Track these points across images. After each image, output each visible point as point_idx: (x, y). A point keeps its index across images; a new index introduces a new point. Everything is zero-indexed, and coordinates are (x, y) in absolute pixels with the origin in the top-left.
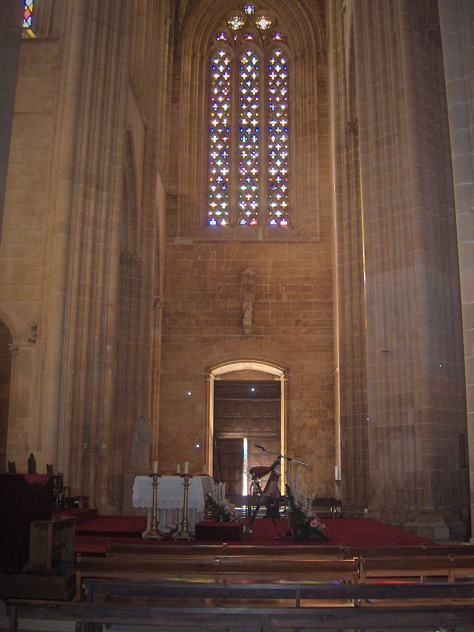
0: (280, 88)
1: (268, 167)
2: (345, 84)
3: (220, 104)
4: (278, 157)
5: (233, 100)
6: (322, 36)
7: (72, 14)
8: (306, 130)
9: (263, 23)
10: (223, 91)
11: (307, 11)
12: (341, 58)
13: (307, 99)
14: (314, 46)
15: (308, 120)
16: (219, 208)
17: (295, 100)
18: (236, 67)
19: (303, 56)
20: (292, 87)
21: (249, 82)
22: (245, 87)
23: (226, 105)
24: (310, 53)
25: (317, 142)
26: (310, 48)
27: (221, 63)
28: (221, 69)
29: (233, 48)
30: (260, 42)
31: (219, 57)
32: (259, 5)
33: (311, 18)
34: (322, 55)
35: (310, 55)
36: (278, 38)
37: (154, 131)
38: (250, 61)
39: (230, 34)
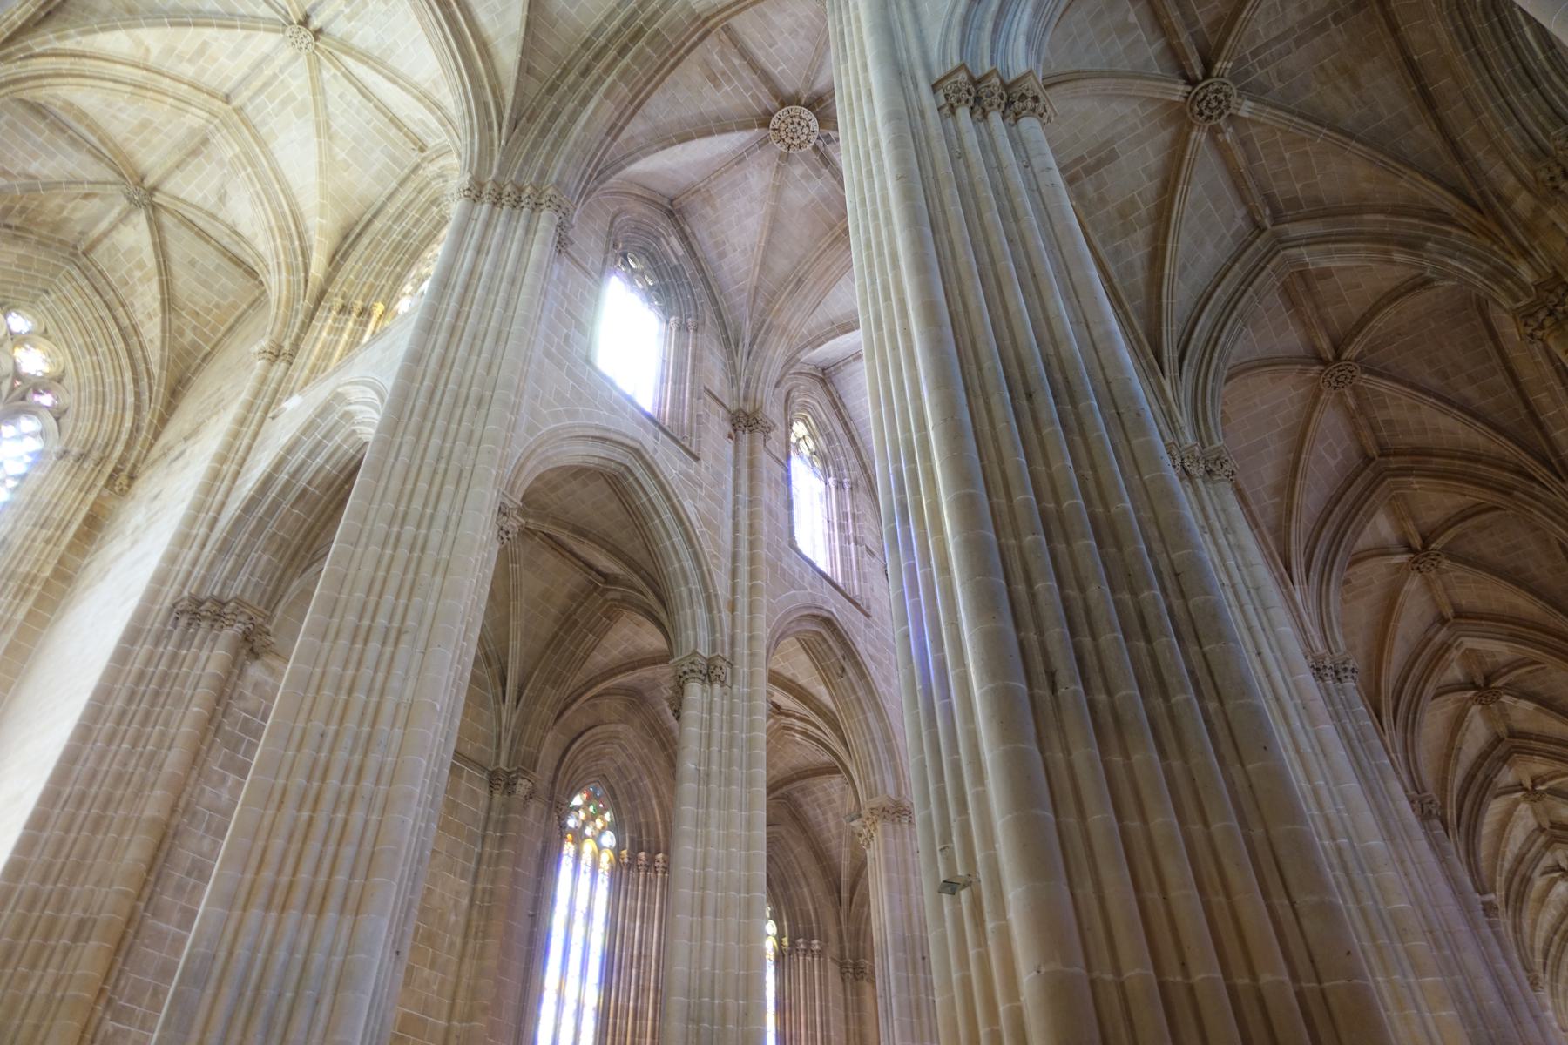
11: (138, 395)
15: (23, 569)
24: (101, 462)
33: (138, 409)
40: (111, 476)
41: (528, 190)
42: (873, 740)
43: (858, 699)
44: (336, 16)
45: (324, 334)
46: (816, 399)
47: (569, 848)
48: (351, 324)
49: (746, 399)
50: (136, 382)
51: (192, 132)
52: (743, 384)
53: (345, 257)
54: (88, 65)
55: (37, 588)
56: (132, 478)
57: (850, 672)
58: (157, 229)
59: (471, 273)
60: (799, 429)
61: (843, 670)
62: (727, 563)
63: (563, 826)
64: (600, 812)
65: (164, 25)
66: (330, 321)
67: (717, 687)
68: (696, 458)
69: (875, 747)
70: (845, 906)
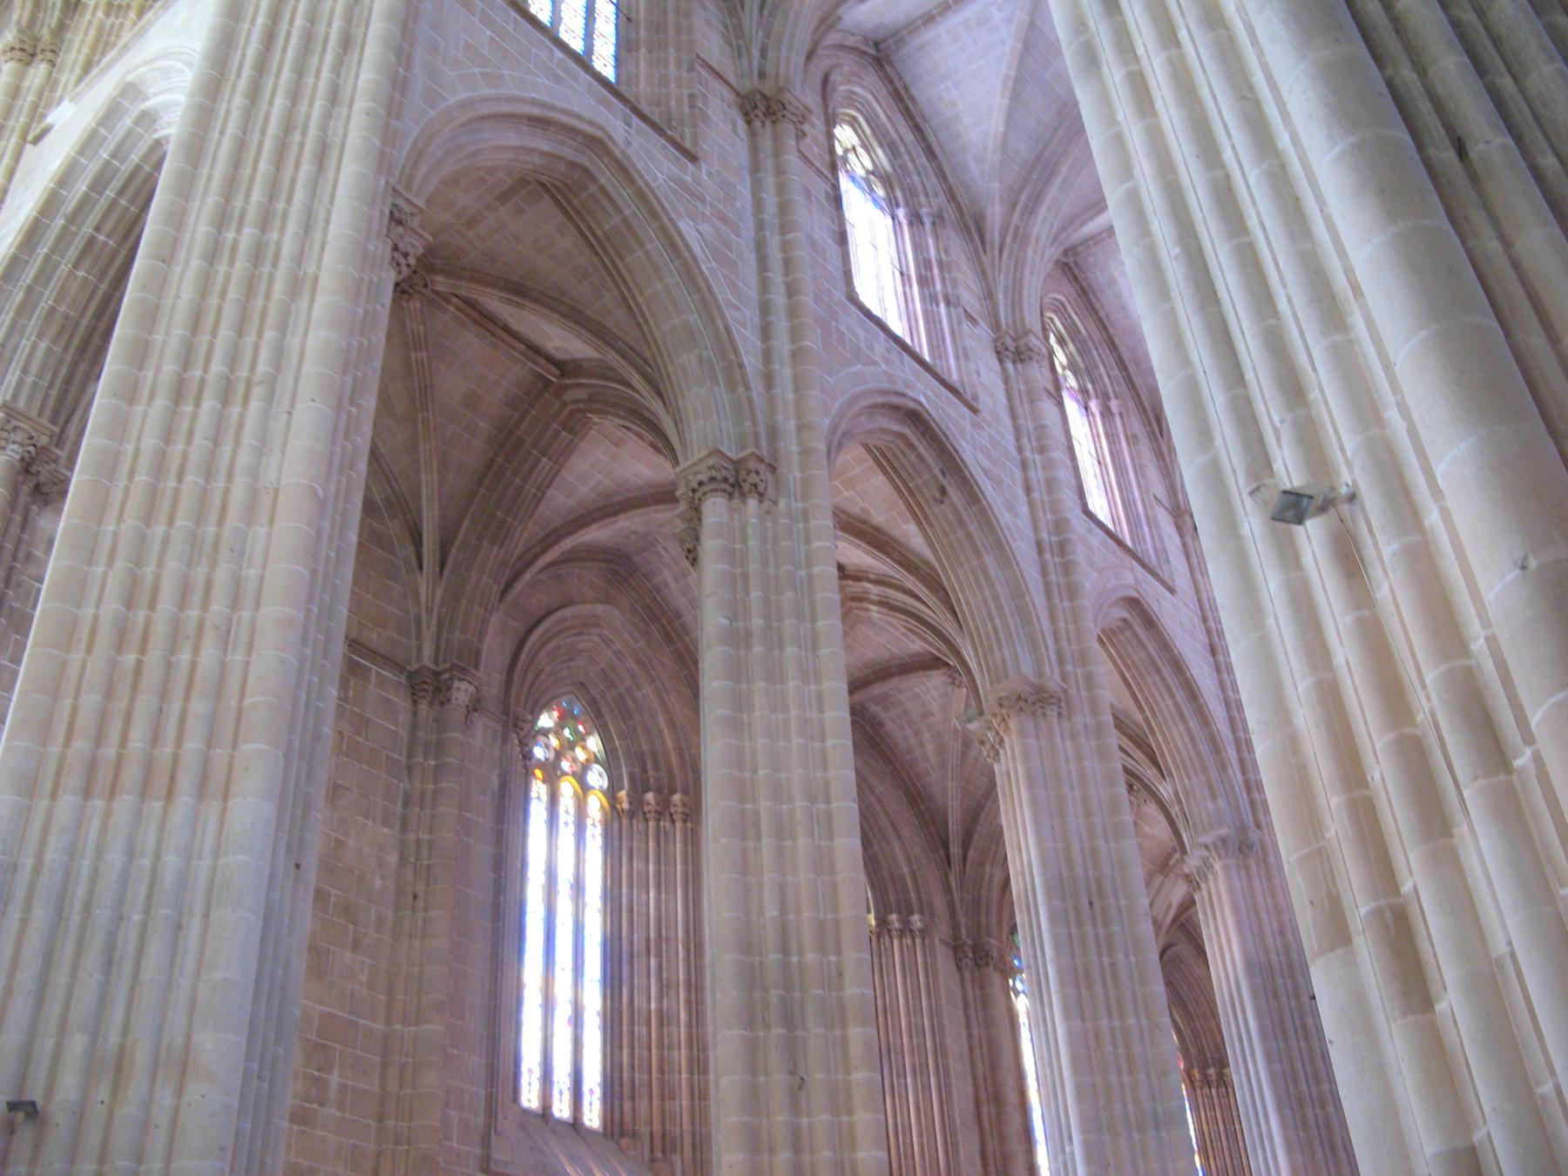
42: (996, 597)
43: (969, 536)
46: (865, 88)
47: (539, 789)
49: (762, 75)
52: (756, 53)
57: (954, 494)
60: (845, 135)
61: (943, 491)
62: (752, 315)
63: (528, 756)
64: (580, 739)
67: (752, 503)
68: (693, 158)
69: (1000, 608)
70: (956, 866)
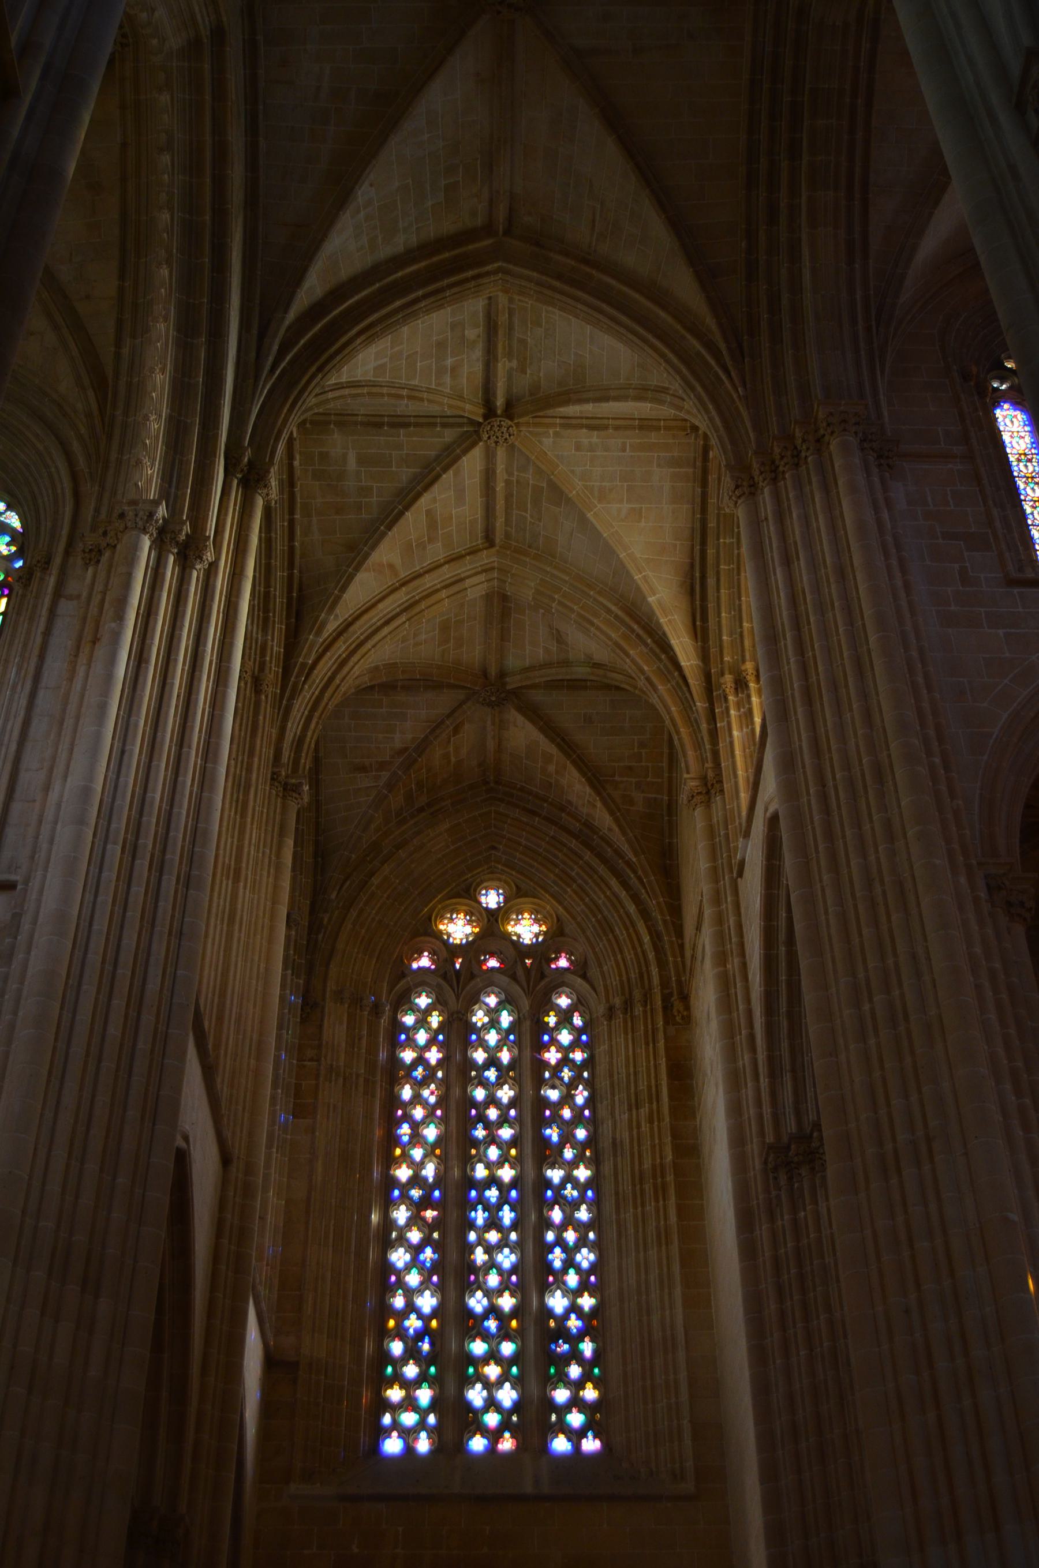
0: (572, 1085)
1: (544, 1288)
2: (753, 1049)
3: (416, 1127)
4: (569, 1263)
5: (453, 1115)
6: (674, 956)
7: (56, 823)
8: (642, 1191)
9: (526, 930)
10: (426, 1093)
11: (635, 898)
12: (738, 985)
13: (644, 1111)
14: (656, 980)
15: (647, 1165)
16: (410, 1403)
17: (613, 1114)
18: (458, 1033)
19: (628, 1005)
20: (603, 1084)
21: (493, 1069)
22: (484, 1083)
23: (432, 1126)
24: (647, 998)
25: (673, 1218)
26: (647, 986)
27: (422, 1022)
28: (422, 1037)
29: (451, 986)
30: (520, 972)
31: (414, 1009)
32: (517, 886)
33: (645, 914)
34: (678, 1005)
35: (646, 1002)
36: (563, 963)
37: (249, 1169)
38: (492, 1018)
39: (445, 954)
40: (665, 1008)
41: (798, 434)
44: (510, 377)
45: (736, 733)
48: (755, 700)
50: (625, 884)
51: (488, 597)
53: (704, 618)
54: (359, 630)
55: (670, 1178)
56: (685, 998)
58: (534, 713)
59: (793, 601)
65: (383, 535)
66: (732, 712)
